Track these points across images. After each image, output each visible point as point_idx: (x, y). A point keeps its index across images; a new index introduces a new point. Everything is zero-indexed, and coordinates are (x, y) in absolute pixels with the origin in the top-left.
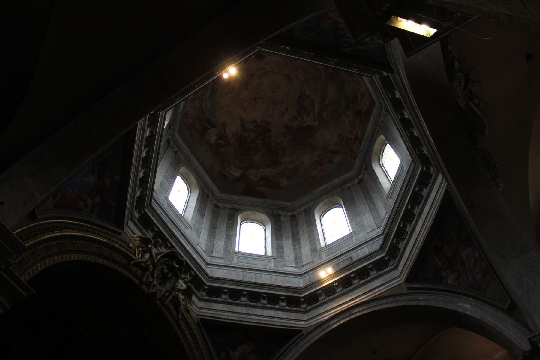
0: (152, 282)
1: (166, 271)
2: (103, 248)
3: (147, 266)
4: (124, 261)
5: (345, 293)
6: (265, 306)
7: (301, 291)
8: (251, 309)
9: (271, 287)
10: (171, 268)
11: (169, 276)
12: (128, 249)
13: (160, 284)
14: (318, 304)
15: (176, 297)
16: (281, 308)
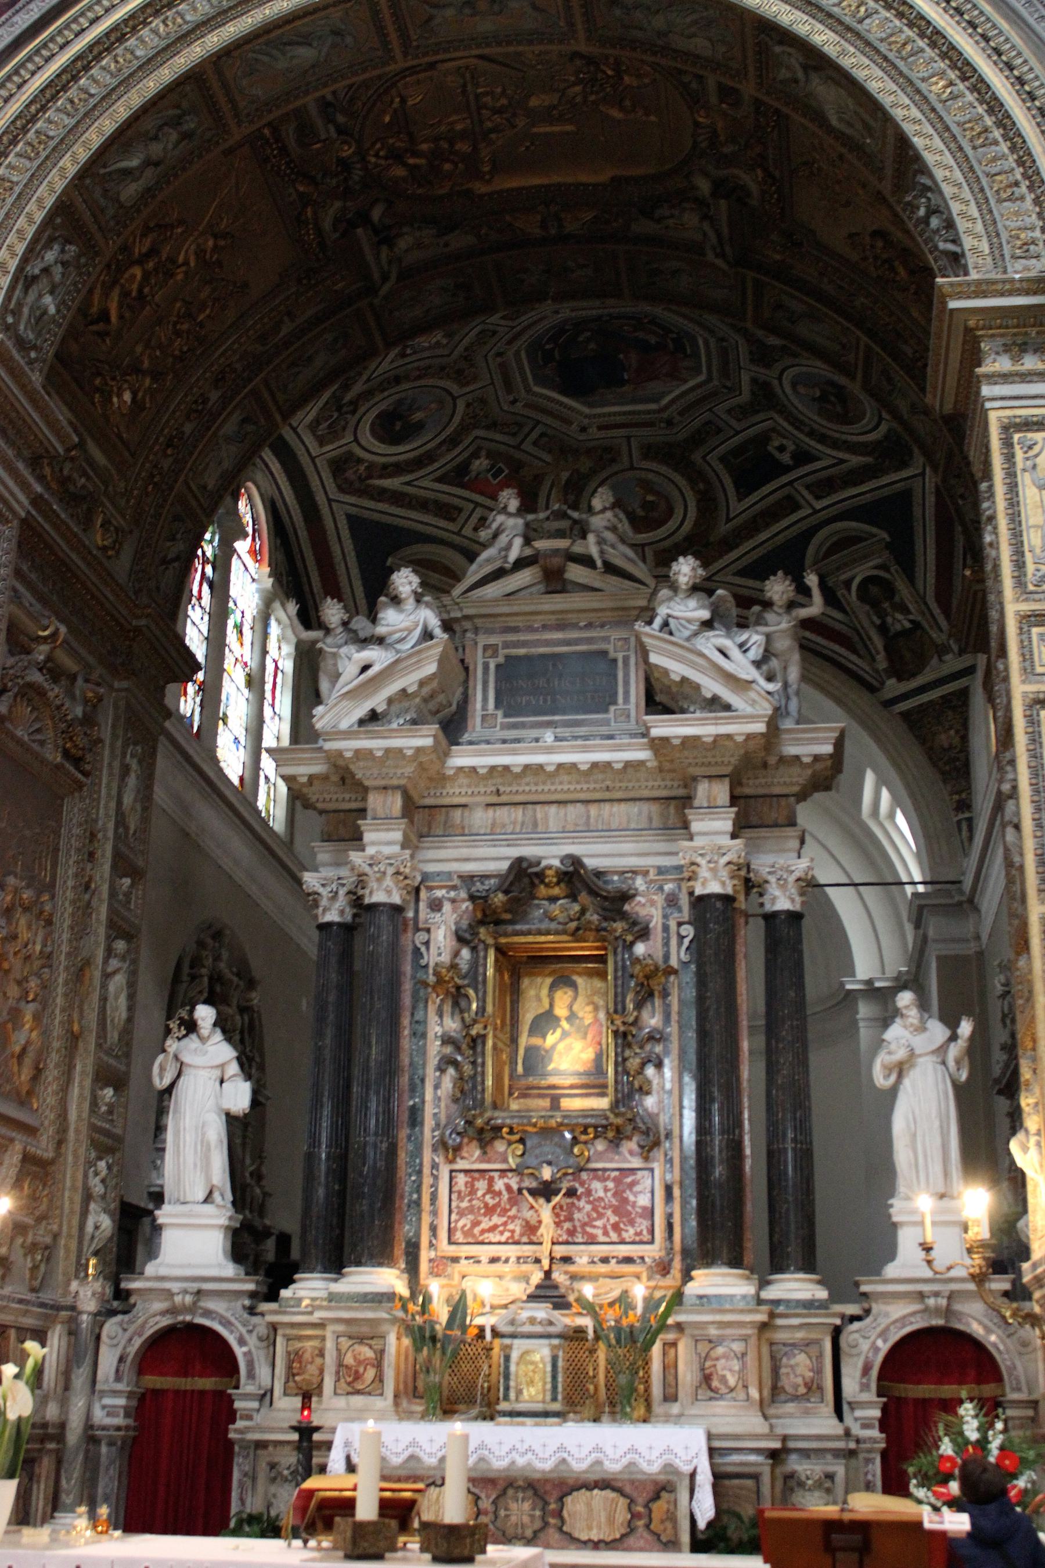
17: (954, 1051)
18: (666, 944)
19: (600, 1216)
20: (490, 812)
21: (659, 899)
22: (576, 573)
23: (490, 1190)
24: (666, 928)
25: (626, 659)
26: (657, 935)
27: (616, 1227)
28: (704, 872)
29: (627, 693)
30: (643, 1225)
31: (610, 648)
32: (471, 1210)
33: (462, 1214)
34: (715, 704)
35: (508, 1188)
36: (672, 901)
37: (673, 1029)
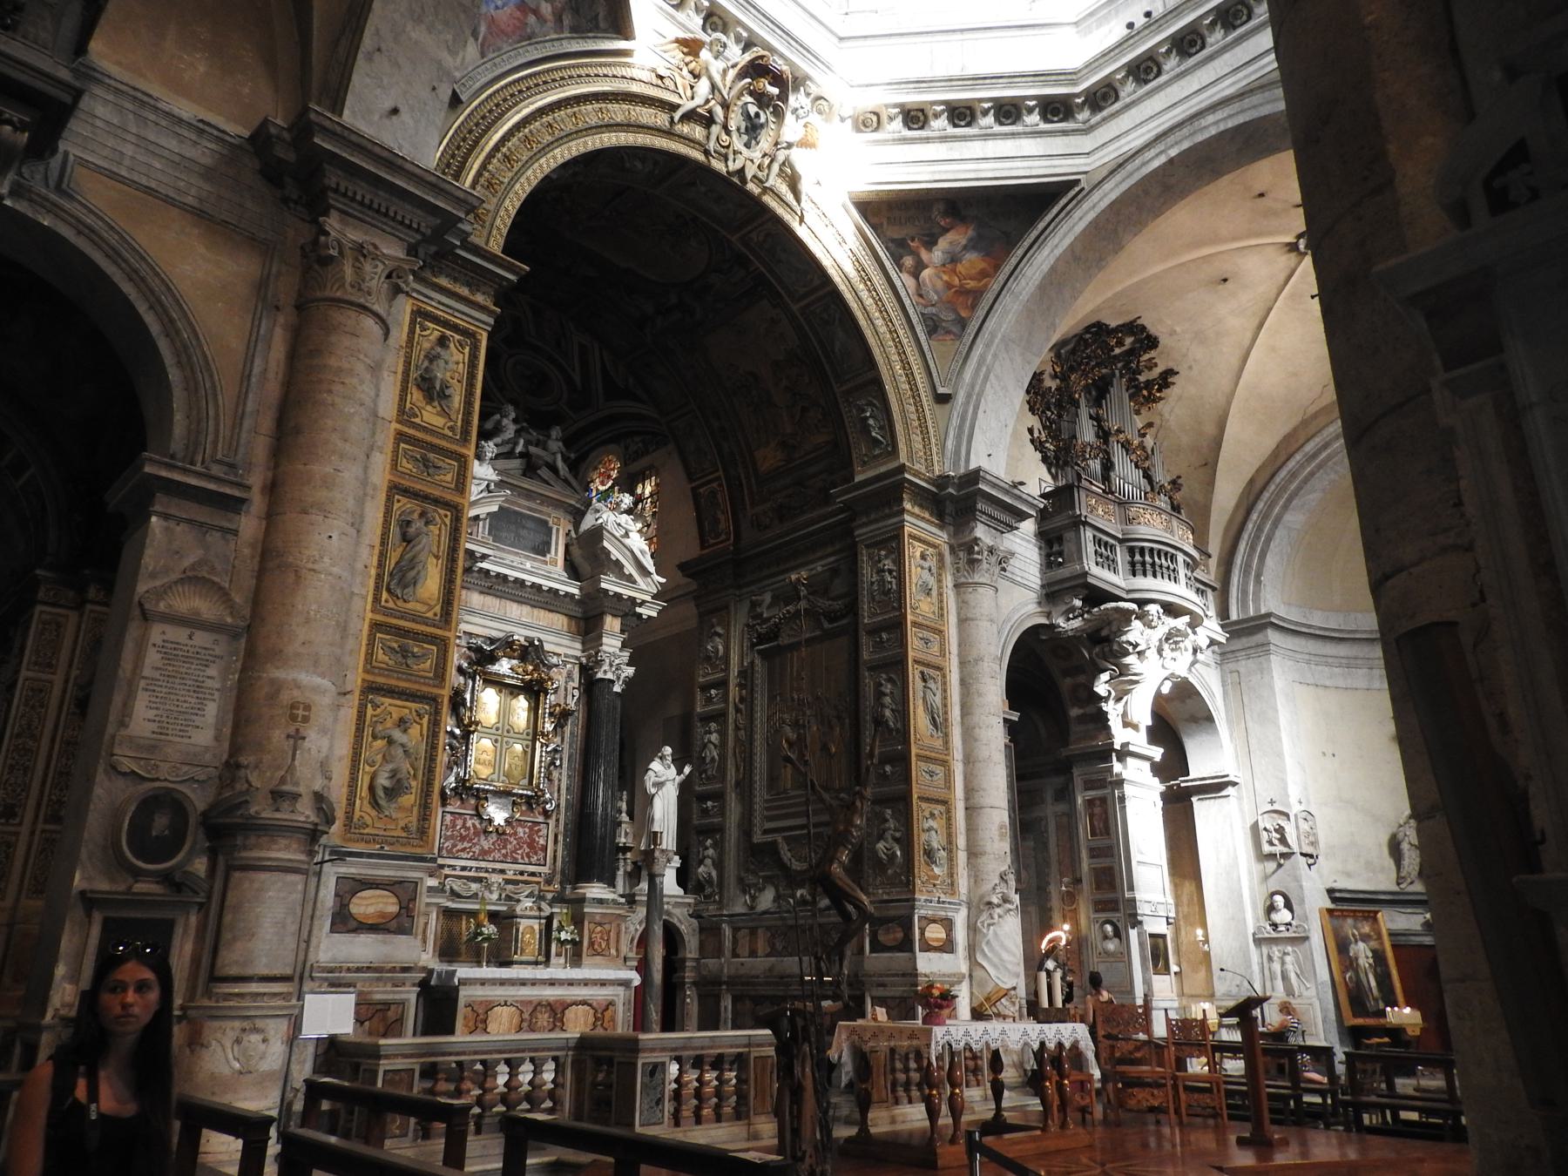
0: (728, 147)
1: (753, 109)
2: (610, 106)
3: (710, 111)
4: (662, 119)
5: (1186, 71)
6: (989, 131)
7: (1074, 77)
8: (957, 144)
9: (1001, 81)
10: (762, 99)
11: (763, 120)
12: (659, 82)
13: (747, 146)
14: (1117, 106)
15: (786, 163)
16: (1028, 129)
17: (679, 779)
18: (566, 698)
19: (521, 848)
20: (482, 596)
21: (565, 673)
22: (544, 472)
23: (464, 826)
24: (566, 689)
25: (558, 530)
26: (562, 692)
27: (529, 857)
28: (606, 667)
29: (556, 549)
30: (541, 855)
31: (551, 521)
32: (452, 837)
33: (447, 839)
34: (630, 579)
35: (474, 825)
36: (569, 676)
37: (566, 746)
